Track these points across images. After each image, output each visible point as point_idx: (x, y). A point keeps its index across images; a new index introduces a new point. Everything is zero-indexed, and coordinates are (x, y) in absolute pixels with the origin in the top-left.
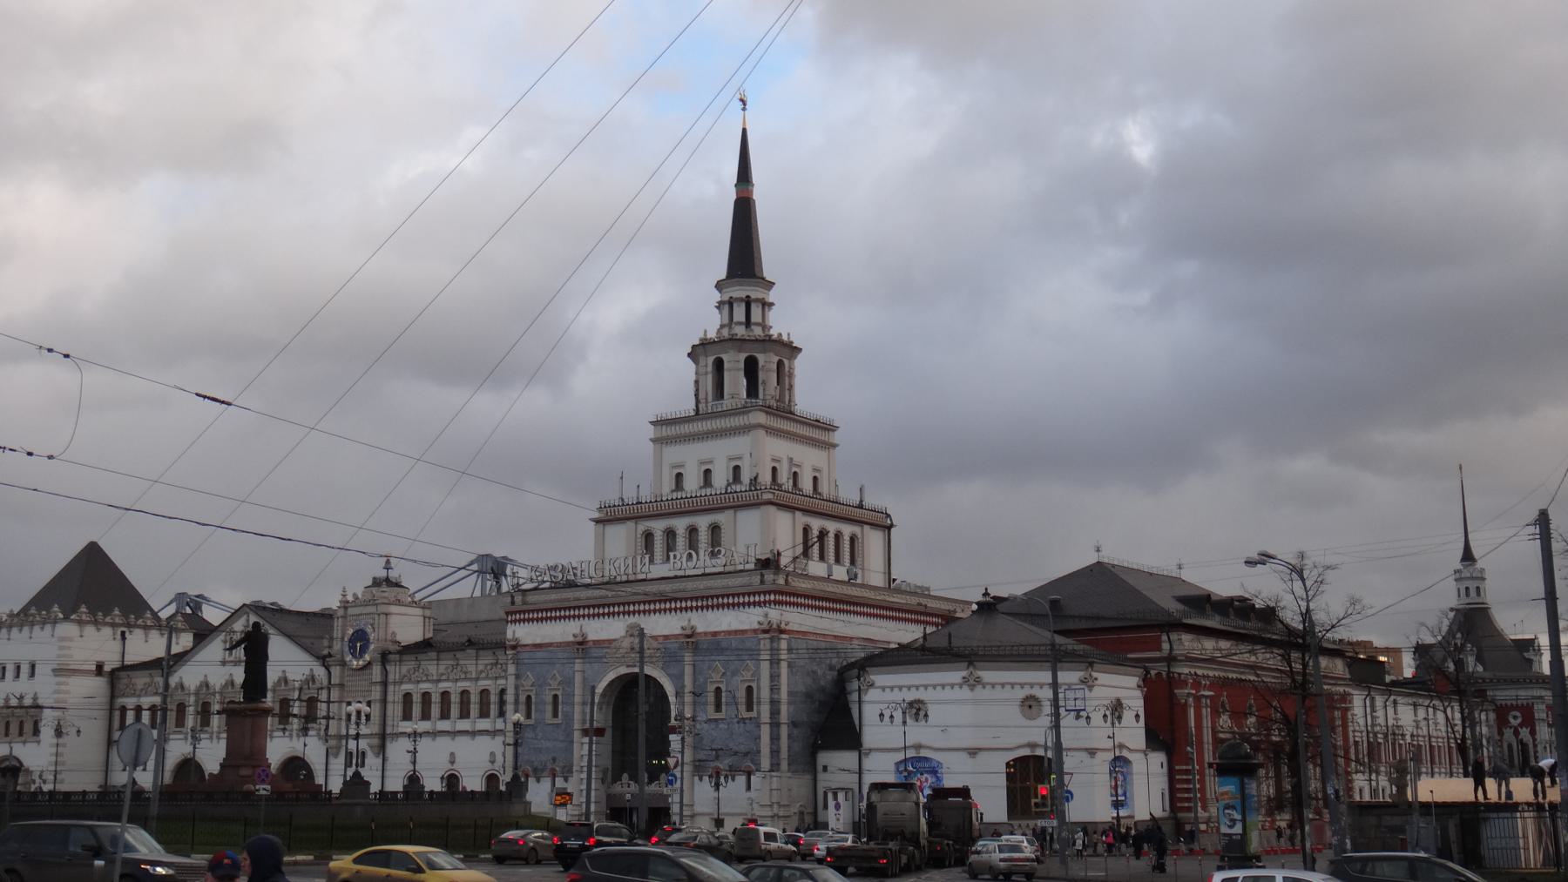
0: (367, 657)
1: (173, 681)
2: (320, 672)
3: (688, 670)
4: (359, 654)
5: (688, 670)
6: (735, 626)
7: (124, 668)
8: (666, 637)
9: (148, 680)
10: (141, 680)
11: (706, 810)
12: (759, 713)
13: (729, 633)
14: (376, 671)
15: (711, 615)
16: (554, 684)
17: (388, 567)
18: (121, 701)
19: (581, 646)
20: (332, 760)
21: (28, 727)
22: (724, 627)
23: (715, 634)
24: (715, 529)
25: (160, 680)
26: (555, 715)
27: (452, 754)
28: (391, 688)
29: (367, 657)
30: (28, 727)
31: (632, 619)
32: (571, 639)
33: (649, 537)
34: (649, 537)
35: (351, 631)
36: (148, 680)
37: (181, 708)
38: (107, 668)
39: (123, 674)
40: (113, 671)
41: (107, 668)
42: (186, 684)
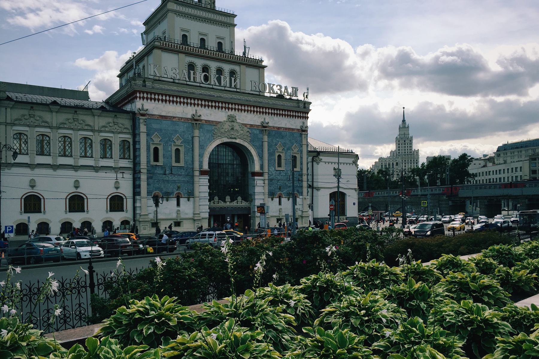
3: (266, 145)
5: (266, 145)
6: (289, 126)
8: (251, 125)
11: (275, 214)
12: (302, 169)
13: (286, 129)
15: (276, 118)
16: (178, 143)
19: (195, 121)
22: (283, 126)
23: (279, 128)
24: (232, 73)
26: (178, 160)
27: (77, 181)
31: (230, 113)
32: (190, 117)
33: (191, 67)
34: (191, 67)
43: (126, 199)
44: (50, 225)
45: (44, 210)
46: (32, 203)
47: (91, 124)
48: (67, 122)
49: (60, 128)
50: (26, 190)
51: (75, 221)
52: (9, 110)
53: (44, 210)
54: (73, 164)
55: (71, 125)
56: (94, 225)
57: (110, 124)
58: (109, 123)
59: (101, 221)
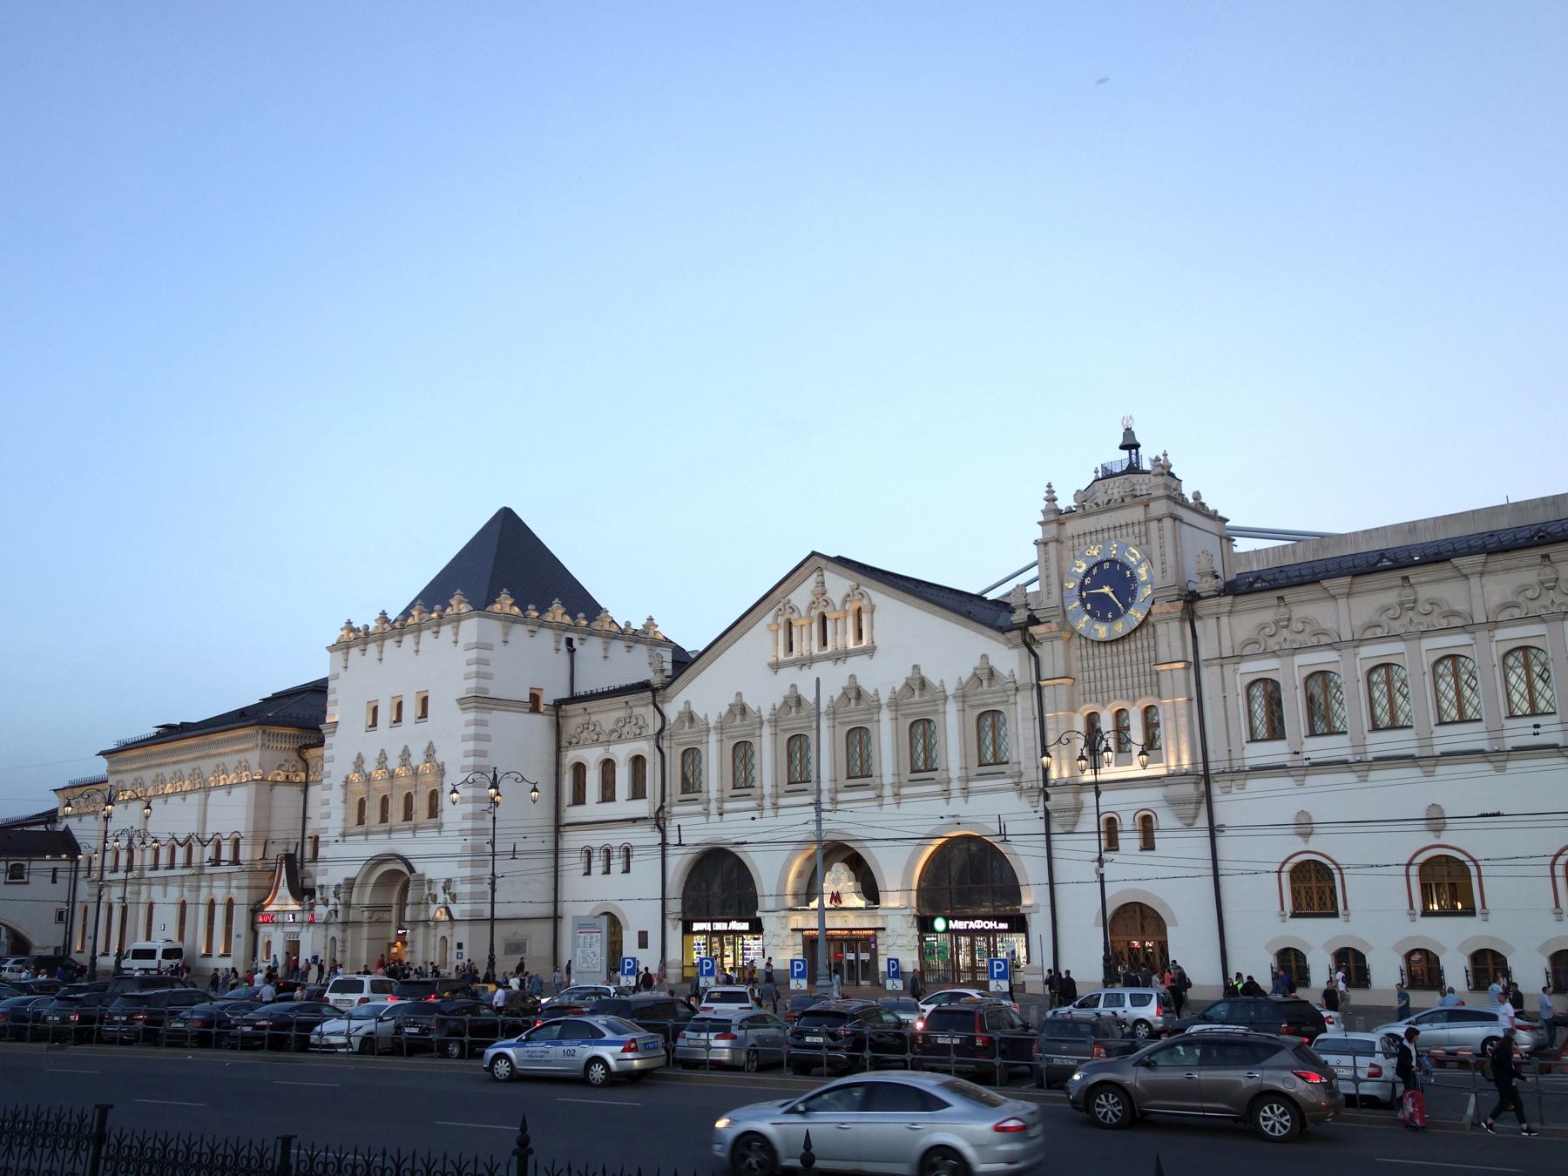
0: (1136, 615)
1: (673, 709)
2: (1007, 659)
4: (1101, 609)
7: (574, 699)
9: (622, 714)
10: (607, 716)
14: (1170, 636)
17: (1130, 445)
18: (571, 757)
20: (1059, 842)
21: (421, 805)
25: (647, 713)
28: (1209, 675)
29: (1136, 615)
30: (421, 805)
35: (1082, 567)
36: (622, 714)
37: (691, 756)
38: (547, 699)
39: (576, 708)
40: (558, 704)
41: (547, 699)
42: (699, 712)
43: (1478, 866)
44: (1370, 960)
45: (1484, 906)
46: (1313, 888)
47: (1460, 607)
48: (1521, 599)
49: (1361, 642)
50: (1289, 847)
51: (1444, 949)
52: (1224, 620)
53: (1484, 906)
54: (1285, 759)
55: (1395, 624)
56: (1311, 960)
57: (1529, 594)
58: (1524, 589)
59: (1541, 950)
